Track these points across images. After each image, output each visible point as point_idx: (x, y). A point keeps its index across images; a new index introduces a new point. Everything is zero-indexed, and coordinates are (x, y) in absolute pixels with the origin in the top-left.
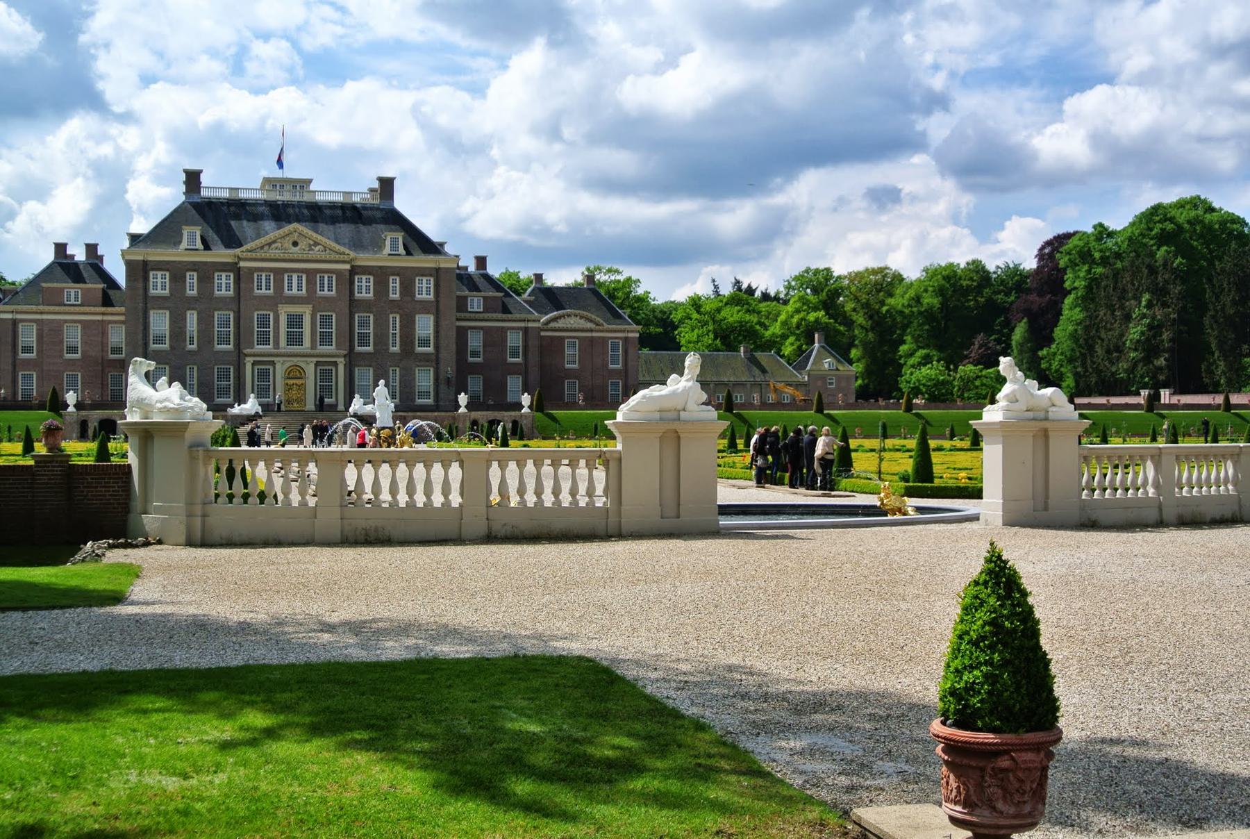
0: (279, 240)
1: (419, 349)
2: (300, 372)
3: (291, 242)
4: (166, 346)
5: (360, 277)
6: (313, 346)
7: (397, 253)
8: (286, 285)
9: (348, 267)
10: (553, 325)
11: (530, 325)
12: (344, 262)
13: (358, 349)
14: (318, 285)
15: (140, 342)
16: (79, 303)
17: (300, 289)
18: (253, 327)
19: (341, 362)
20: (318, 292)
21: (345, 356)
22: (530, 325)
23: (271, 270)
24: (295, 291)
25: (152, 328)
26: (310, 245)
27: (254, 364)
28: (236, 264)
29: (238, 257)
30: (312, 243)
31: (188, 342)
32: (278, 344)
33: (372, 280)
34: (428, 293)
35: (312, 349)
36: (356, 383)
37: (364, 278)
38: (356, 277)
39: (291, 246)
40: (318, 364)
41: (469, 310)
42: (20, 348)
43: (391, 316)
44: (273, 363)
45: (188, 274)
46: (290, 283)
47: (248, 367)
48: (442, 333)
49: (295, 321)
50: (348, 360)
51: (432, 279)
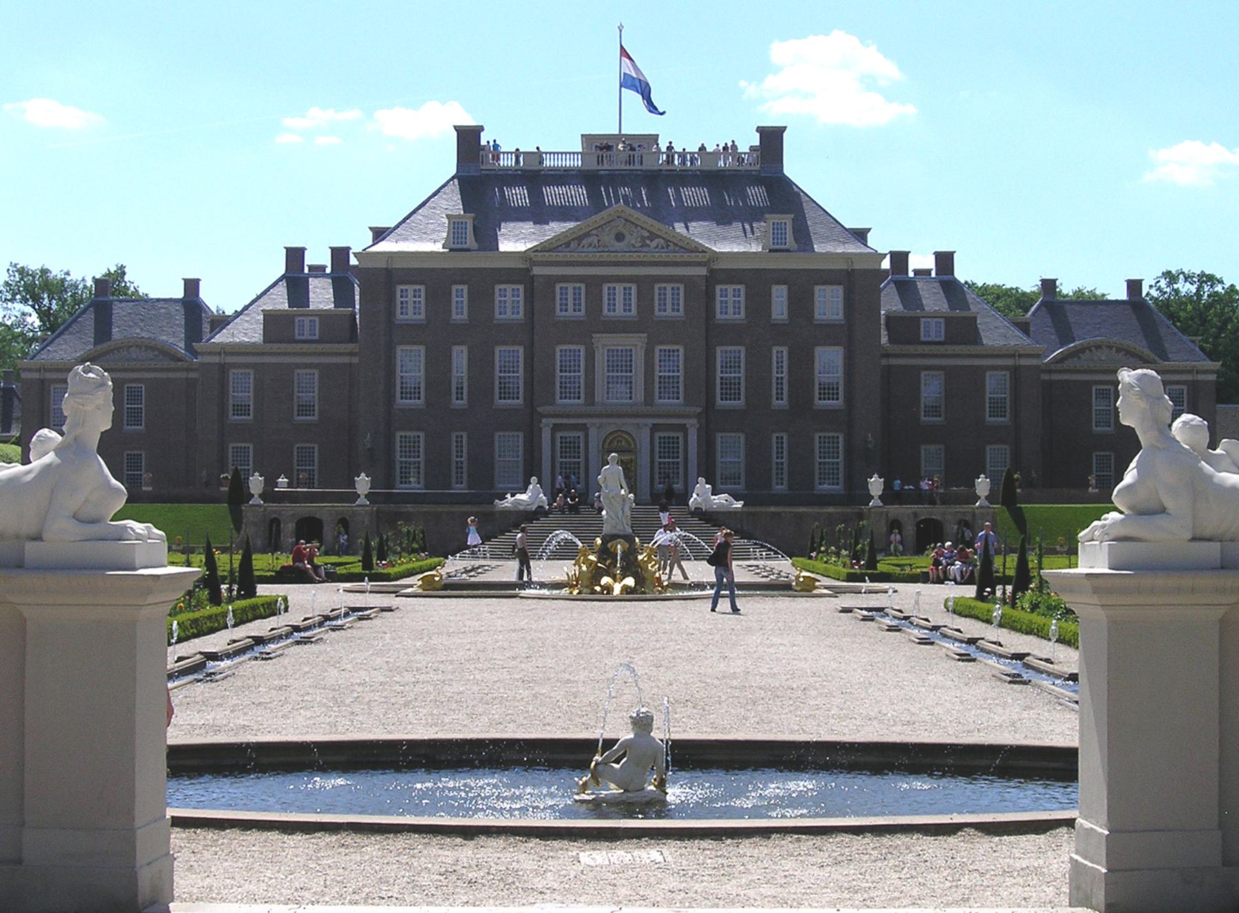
1: (820, 403)
2: (627, 442)
3: (613, 236)
4: (420, 402)
5: (724, 287)
7: (783, 247)
9: (703, 271)
11: (1023, 362)
12: (699, 264)
14: (656, 302)
16: (316, 337)
19: (692, 425)
20: (657, 313)
21: (698, 416)
23: (580, 279)
24: (619, 311)
26: (643, 238)
27: (556, 428)
28: (528, 270)
29: (531, 259)
31: (454, 397)
32: (593, 396)
33: (742, 293)
36: (719, 459)
37: (730, 288)
38: (718, 288)
39: (613, 242)
40: (655, 428)
41: (923, 339)
42: (231, 408)
45: (454, 287)
46: (612, 299)
47: (546, 434)
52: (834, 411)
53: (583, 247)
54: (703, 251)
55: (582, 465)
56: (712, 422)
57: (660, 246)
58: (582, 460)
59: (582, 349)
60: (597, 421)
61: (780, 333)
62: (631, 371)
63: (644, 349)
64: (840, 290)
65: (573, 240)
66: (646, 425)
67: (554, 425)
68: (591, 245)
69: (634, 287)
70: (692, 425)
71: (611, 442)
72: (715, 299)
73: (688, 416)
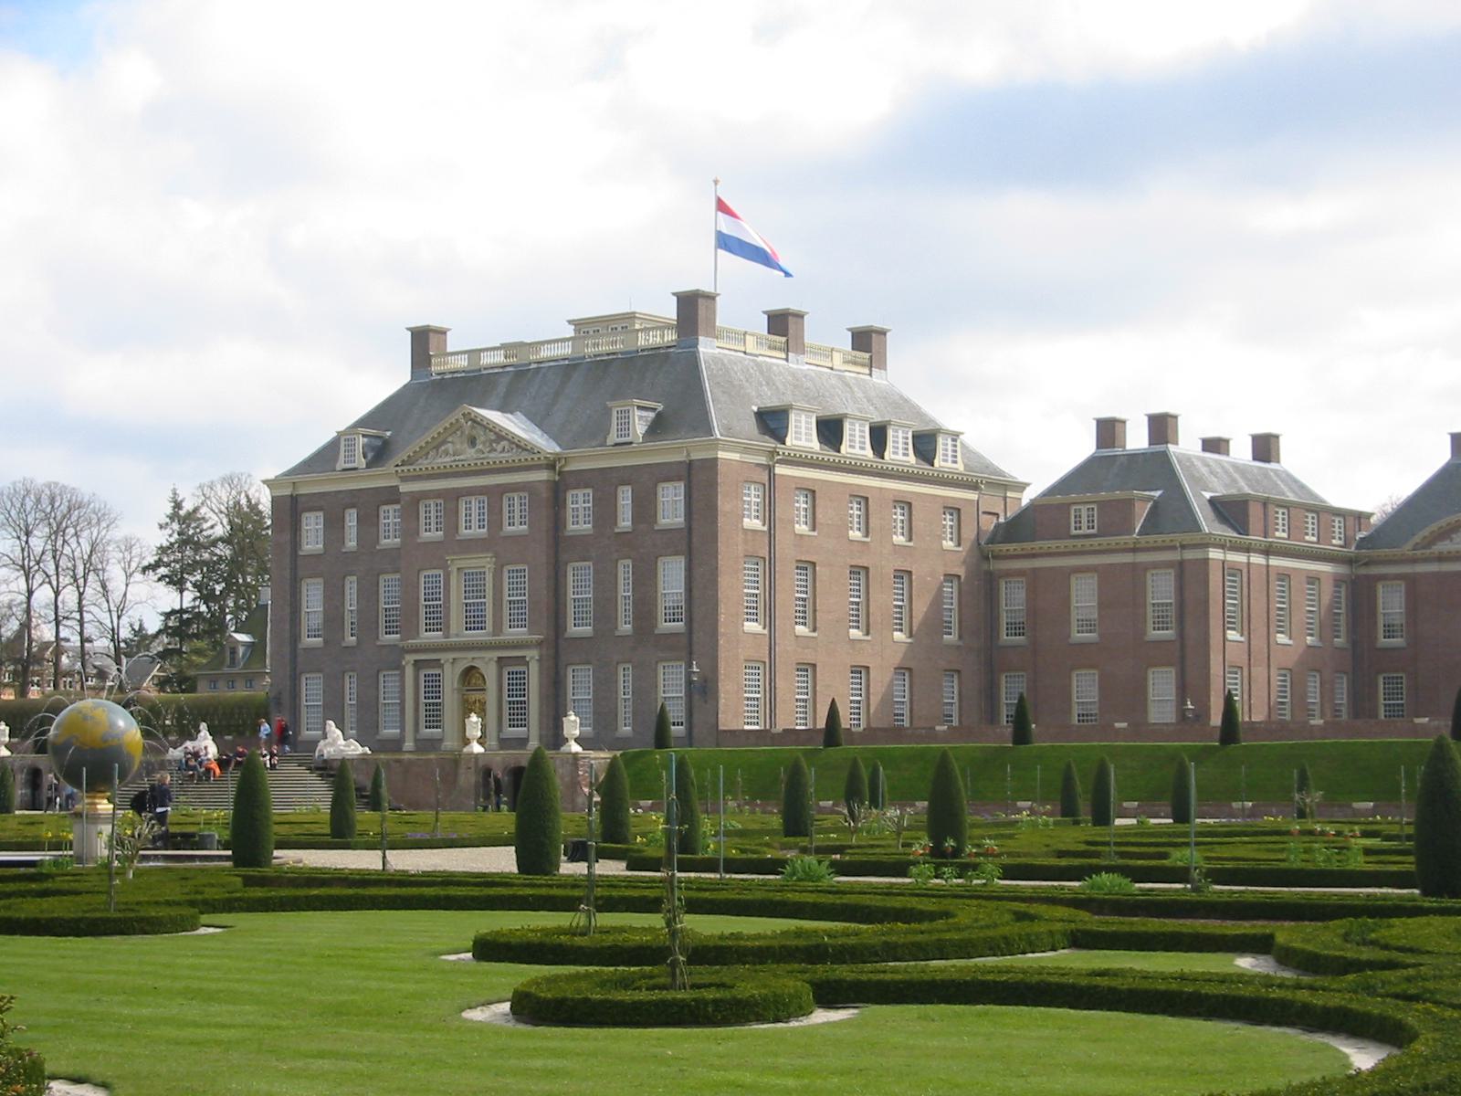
0: (450, 439)
6: (498, 628)
8: (462, 518)
9: (543, 476)
10: (1444, 547)
13: (574, 630)
15: (287, 635)
18: (418, 599)
19: (532, 654)
25: (304, 609)
30: (493, 437)
37: (580, 493)
41: (1074, 532)
47: (409, 671)
48: (696, 593)
49: (473, 583)
52: (676, 634)
56: (557, 650)
60: (451, 656)
61: (626, 542)
64: (681, 486)
66: (491, 659)
67: (415, 661)
70: (532, 658)
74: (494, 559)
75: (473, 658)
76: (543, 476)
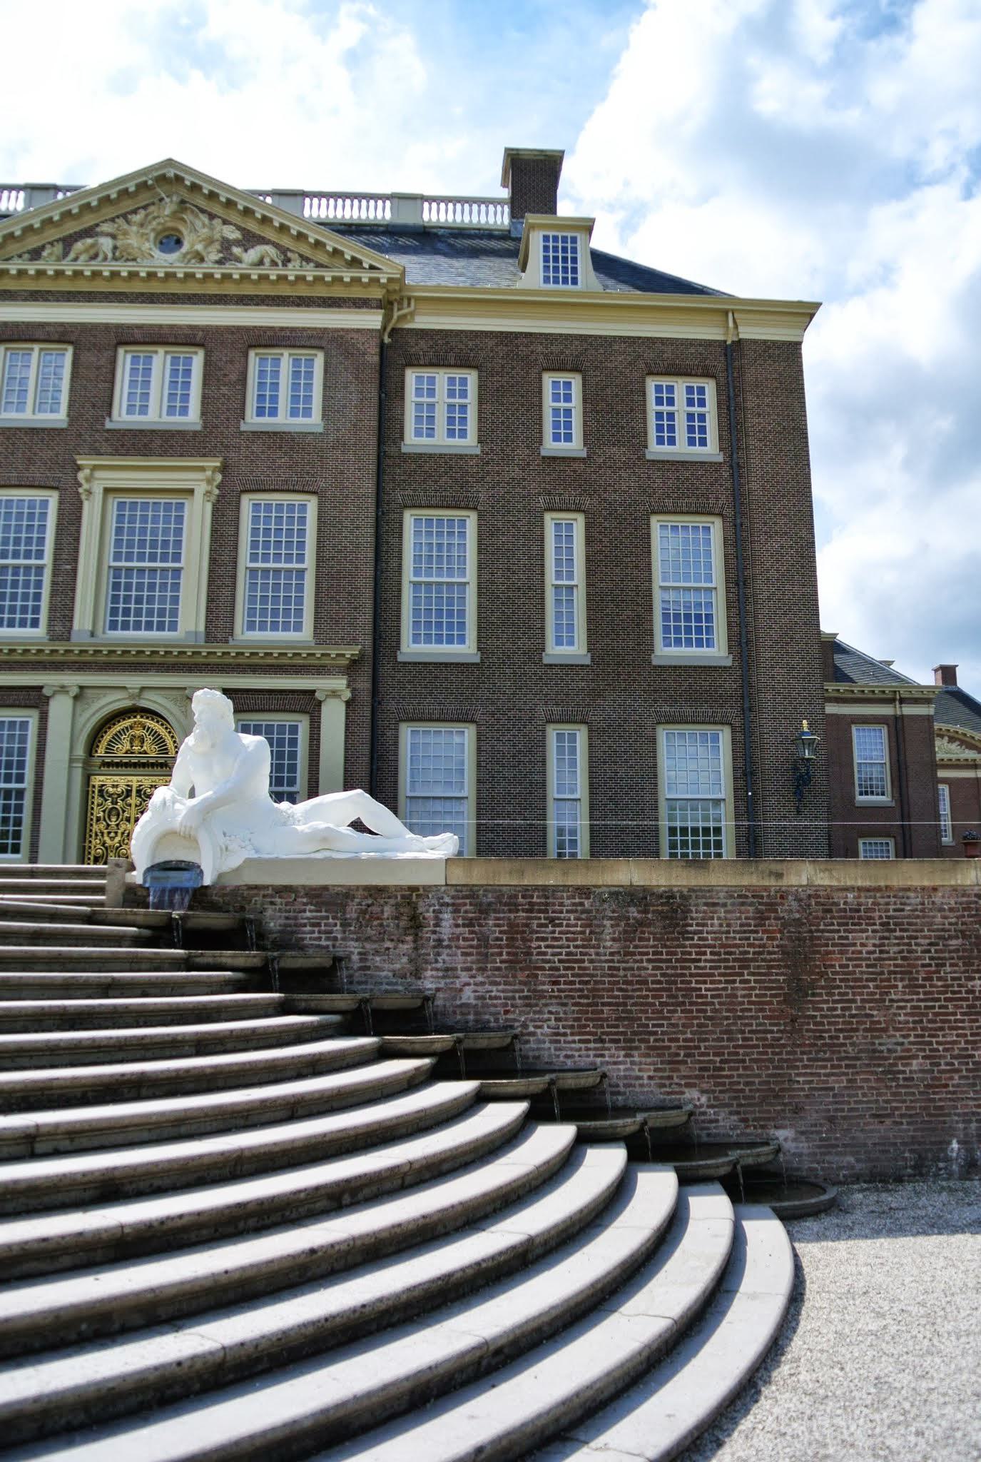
0: (106, 228)
1: (666, 652)
2: (158, 739)
5: (426, 373)
9: (372, 320)
11: (908, 710)
13: (412, 648)
17: (177, 402)
21: (352, 668)
22: (908, 710)
24: (156, 415)
26: (226, 245)
30: (237, 235)
34: (696, 435)
35: (210, 636)
37: (442, 377)
38: (411, 376)
43: (550, 520)
44: (36, 699)
50: (364, 684)
51: (710, 387)
53: (76, 259)
54: (372, 267)
55: (28, 802)
57: (267, 261)
58: (28, 784)
59: (53, 498)
60: (73, 680)
62: (177, 557)
63: (213, 498)
65: (51, 244)
68: (95, 257)
69: (198, 361)
70: (334, 694)
71: (117, 736)
72: (403, 398)
73: (320, 670)
74: (219, 477)
75: (143, 689)
76: (372, 320)
